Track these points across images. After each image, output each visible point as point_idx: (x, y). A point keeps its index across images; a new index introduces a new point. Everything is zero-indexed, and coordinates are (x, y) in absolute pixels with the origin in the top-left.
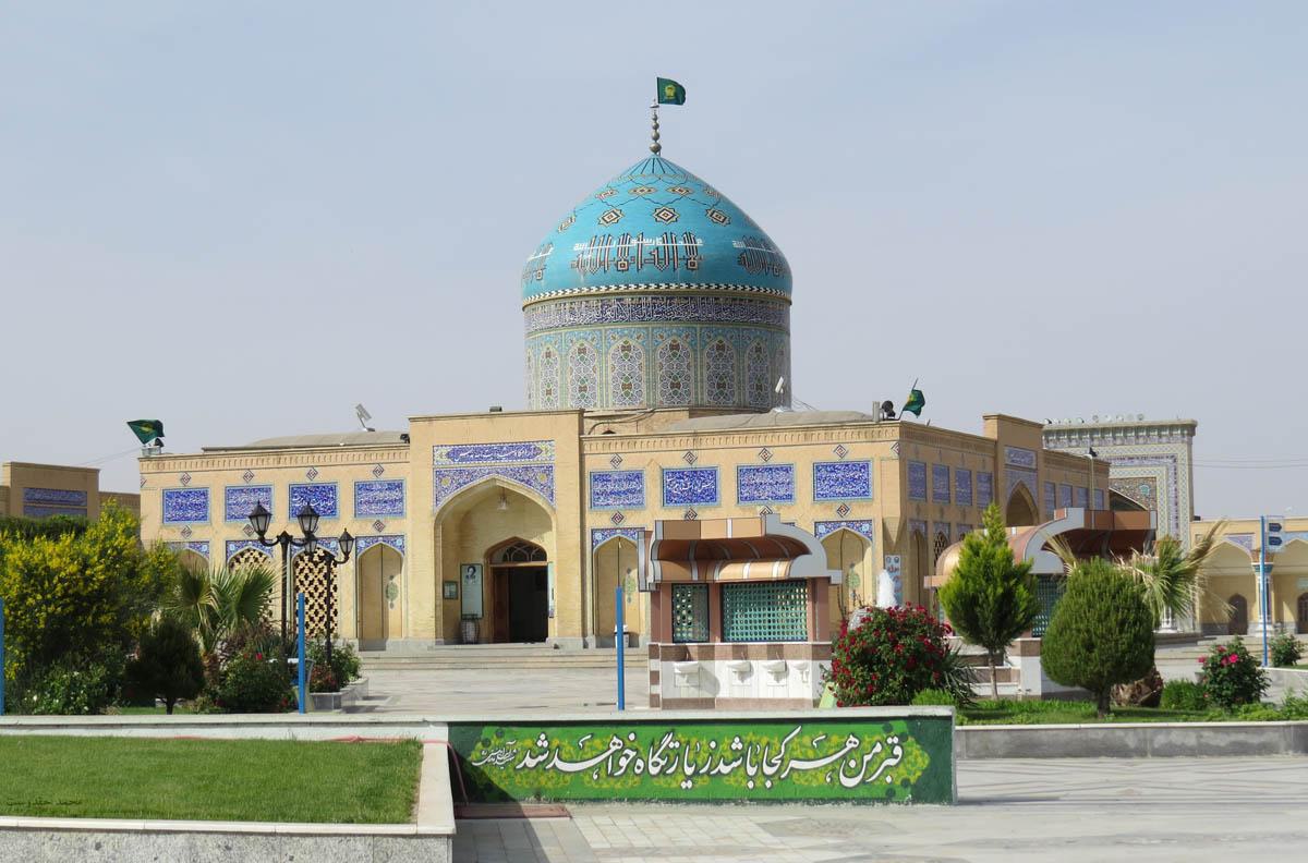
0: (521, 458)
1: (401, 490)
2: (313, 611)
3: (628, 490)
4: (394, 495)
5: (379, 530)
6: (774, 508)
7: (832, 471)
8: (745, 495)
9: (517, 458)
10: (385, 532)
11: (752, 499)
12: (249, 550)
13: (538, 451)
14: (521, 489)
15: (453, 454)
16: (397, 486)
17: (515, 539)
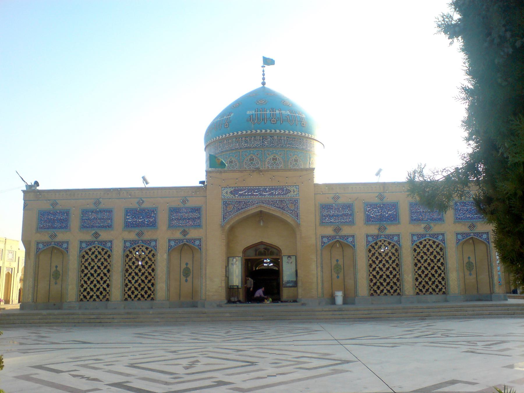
0: (278, 195)
1: (199, 213)
2: (137, 284)
3: (343, 214)
4: (196, 215)
5: (185, 235)
6: (432, 225)
7: (464, 206)
8: (414, 218)
9: (275, 195)
10: (188, 237)
11: (419, 220)
12: (95, 247)
13: (289, 191)
14: (277, 213)
15: (234, 192)
16: (198, 210)
17: (262, 243)
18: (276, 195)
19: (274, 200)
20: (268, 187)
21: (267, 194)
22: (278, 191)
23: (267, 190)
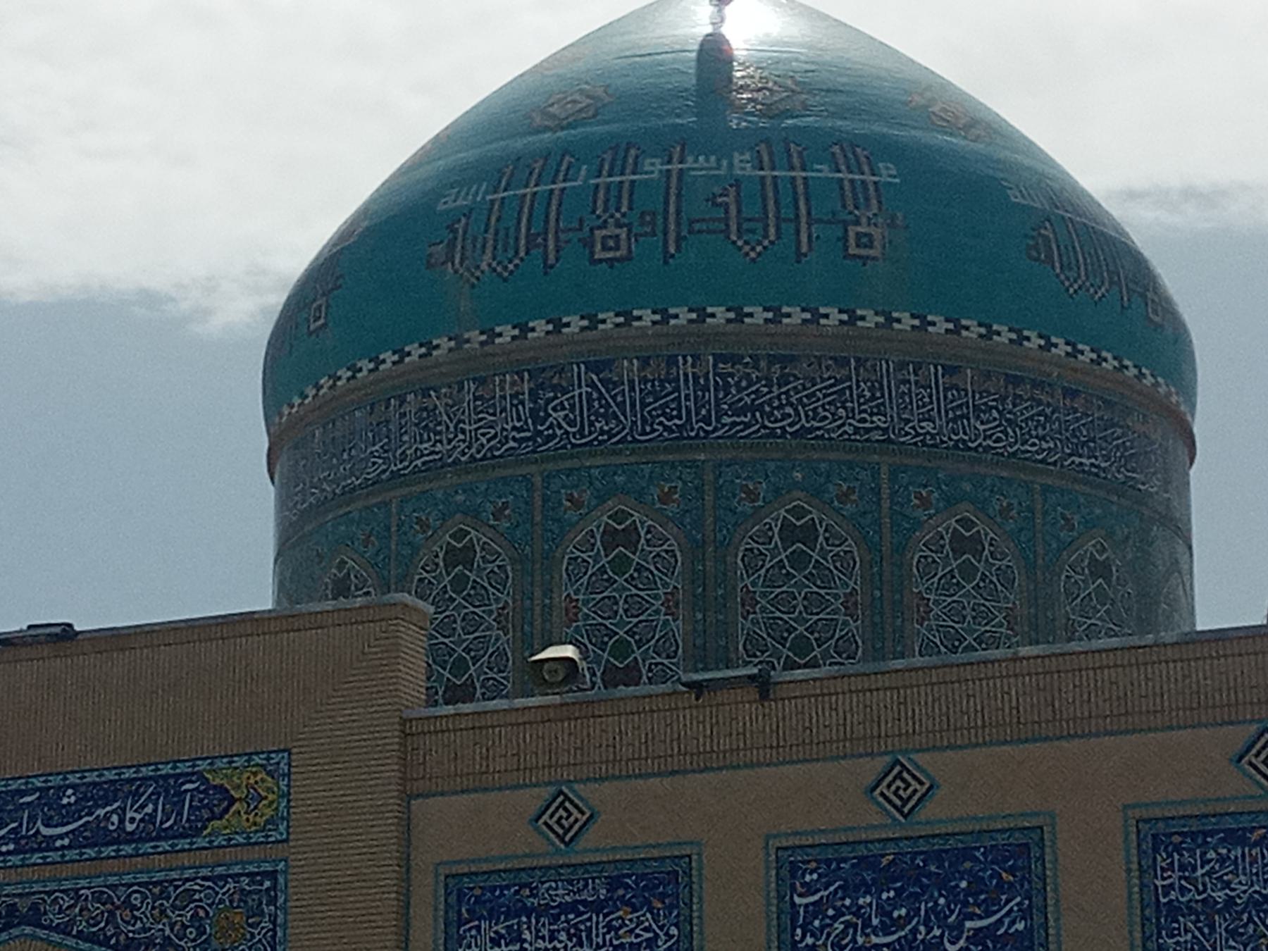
18: (131, 838)
19: (113, 880)
20: (72, 779)
21: (61, 837)
22: (143, 806)
23: (69, 798)
